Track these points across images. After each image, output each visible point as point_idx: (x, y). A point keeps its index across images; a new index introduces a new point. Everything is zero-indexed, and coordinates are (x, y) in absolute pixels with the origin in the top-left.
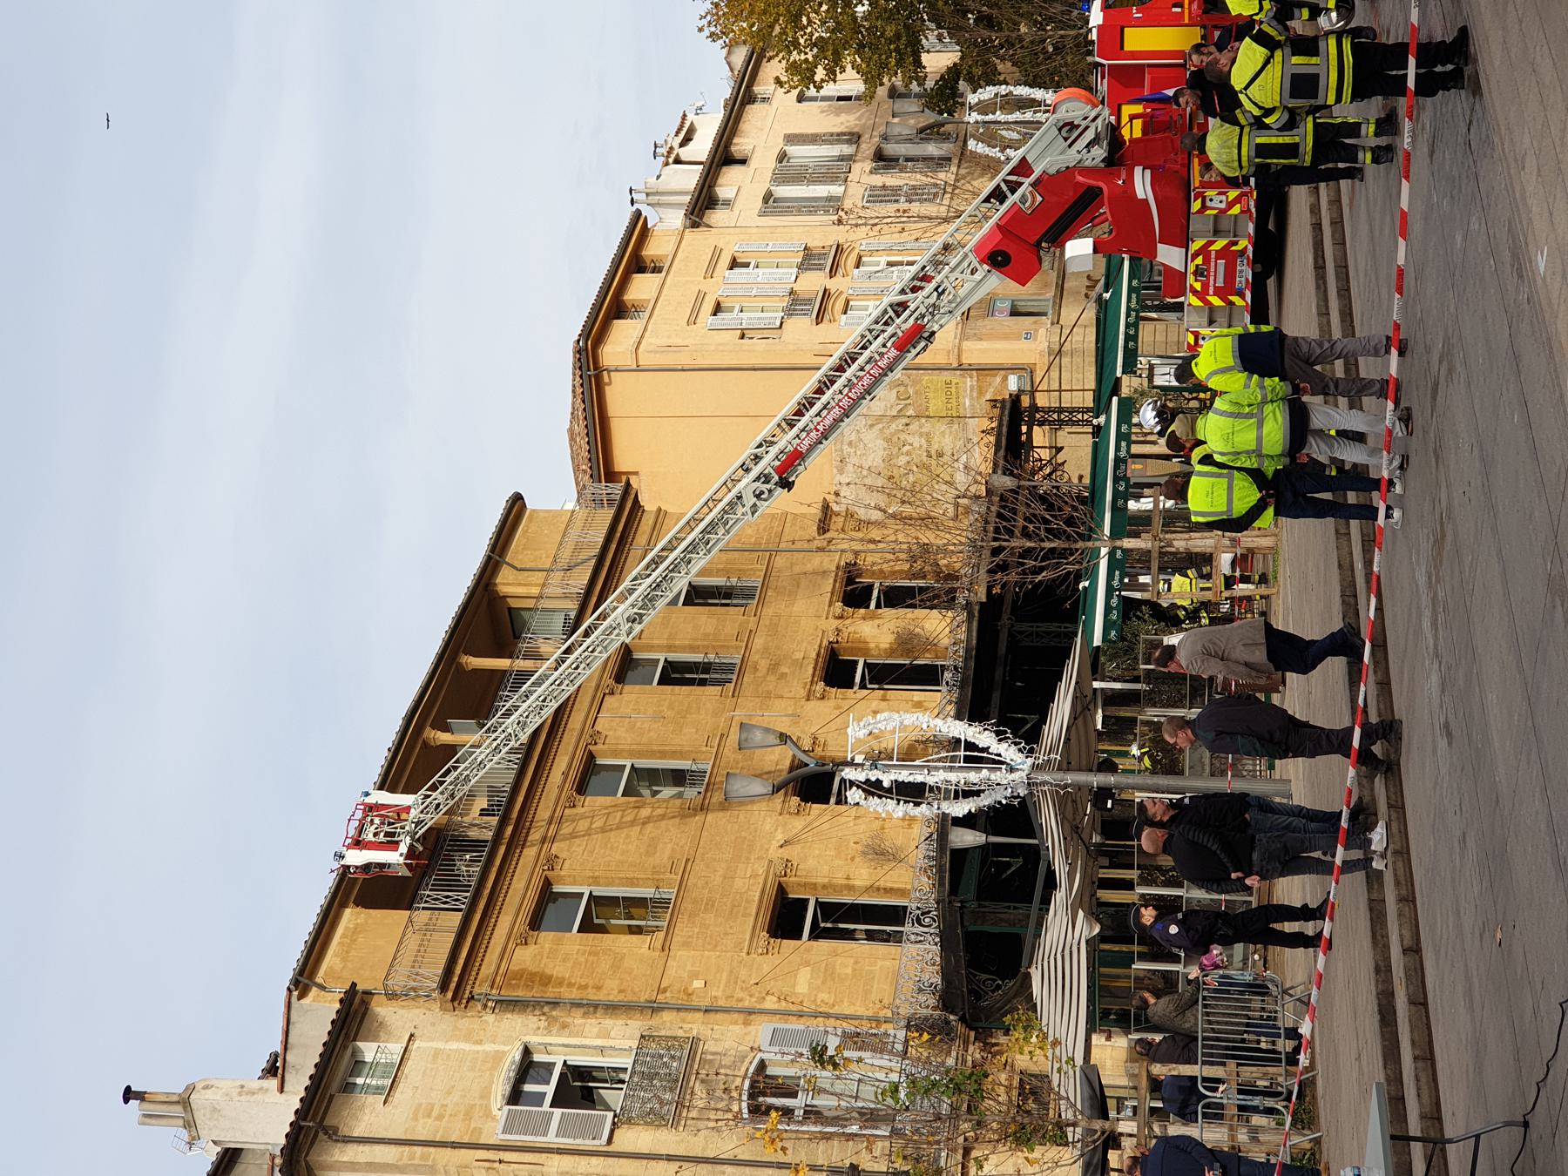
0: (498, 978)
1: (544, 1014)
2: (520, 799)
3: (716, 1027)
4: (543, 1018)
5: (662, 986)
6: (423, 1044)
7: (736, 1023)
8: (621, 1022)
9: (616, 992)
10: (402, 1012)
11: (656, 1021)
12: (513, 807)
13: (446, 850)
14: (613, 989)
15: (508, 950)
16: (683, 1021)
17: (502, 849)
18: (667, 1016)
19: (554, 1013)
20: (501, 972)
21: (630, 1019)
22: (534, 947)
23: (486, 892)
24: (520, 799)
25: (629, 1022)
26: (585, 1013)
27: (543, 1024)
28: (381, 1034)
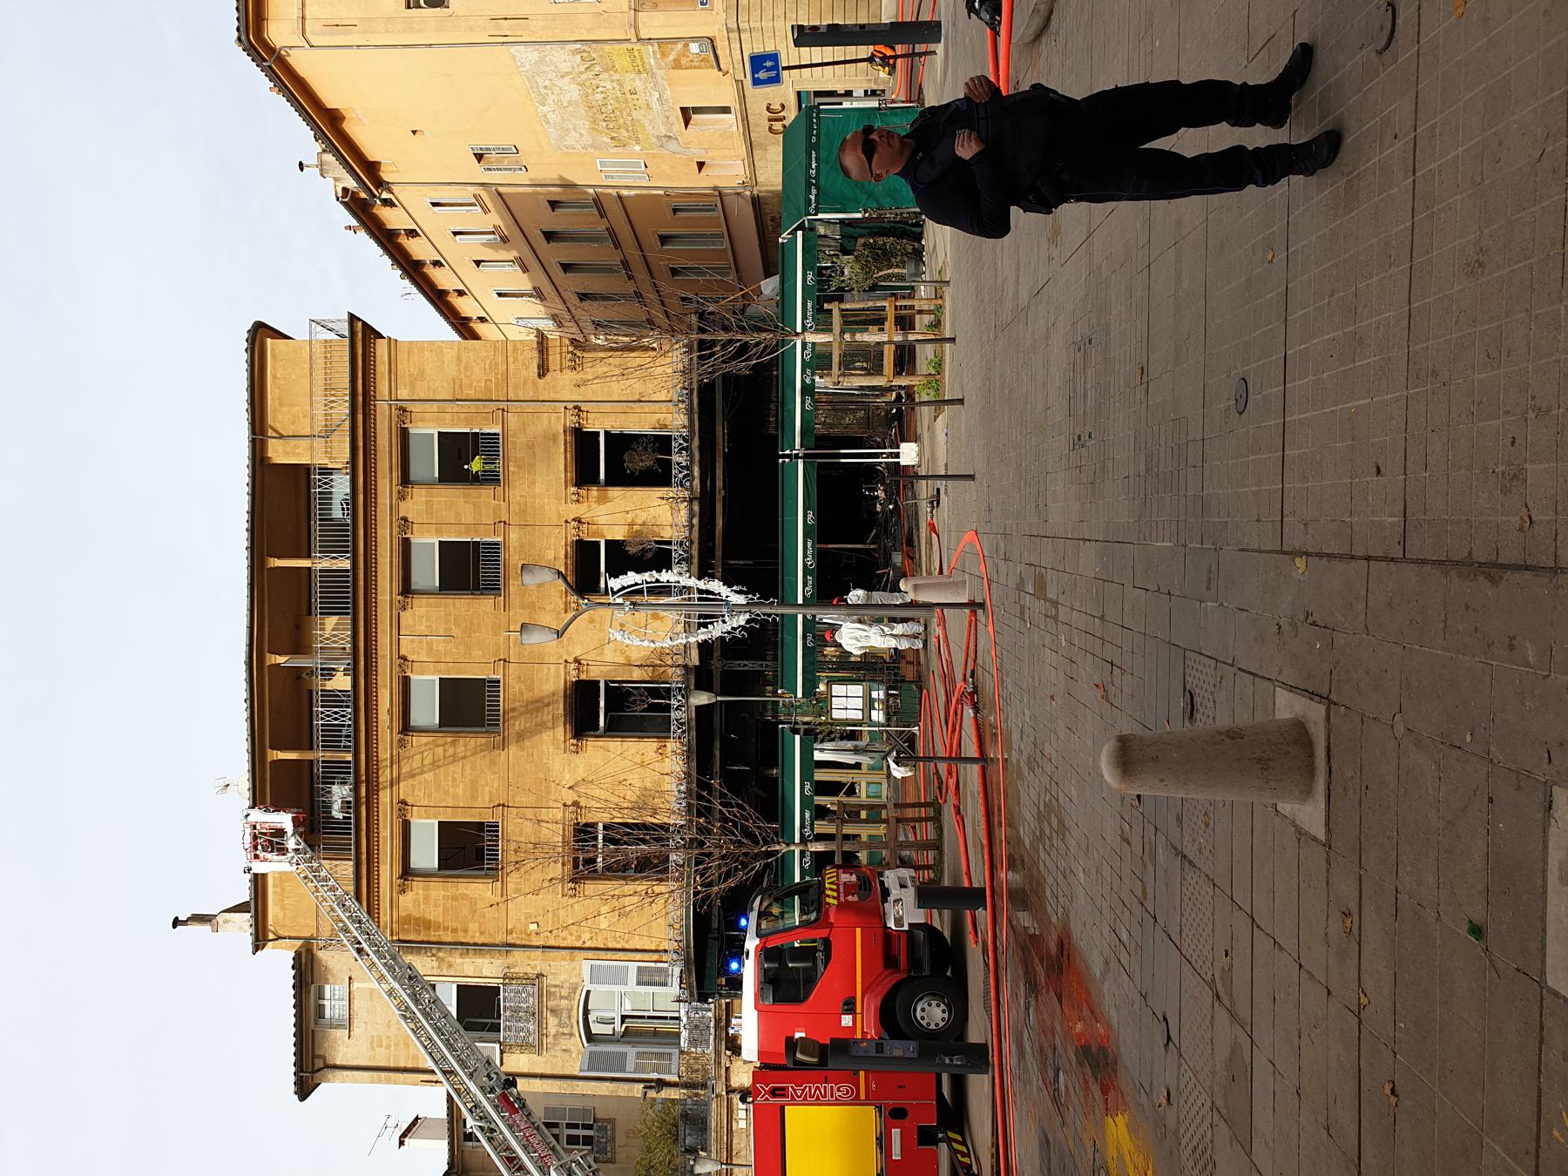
0: (394, 925)
1: (433, 955)
2: (363, 756)
3: (552, 963)
4: (434, 958)
5: (509, 928)
6: (360, 985)
7: (564, 959)
8: (487, 961)
9: (478, 934)
10: (336, 957)
11: (510, 960)
12: (360, 767)
13: (323, 817)
14: (475, 932)
15: (394, 898)
16: (529, 958)
17: (363, 808)
18: (518, 955)
19: (441, 954)
20: (394, 919)
21: (493, 958)
22: (412, 893)
23: (364, 857)
24: (363, 756)
25: (493, 960)
26: (461, 954)
27: (435, 964)
28: (329, 977)
